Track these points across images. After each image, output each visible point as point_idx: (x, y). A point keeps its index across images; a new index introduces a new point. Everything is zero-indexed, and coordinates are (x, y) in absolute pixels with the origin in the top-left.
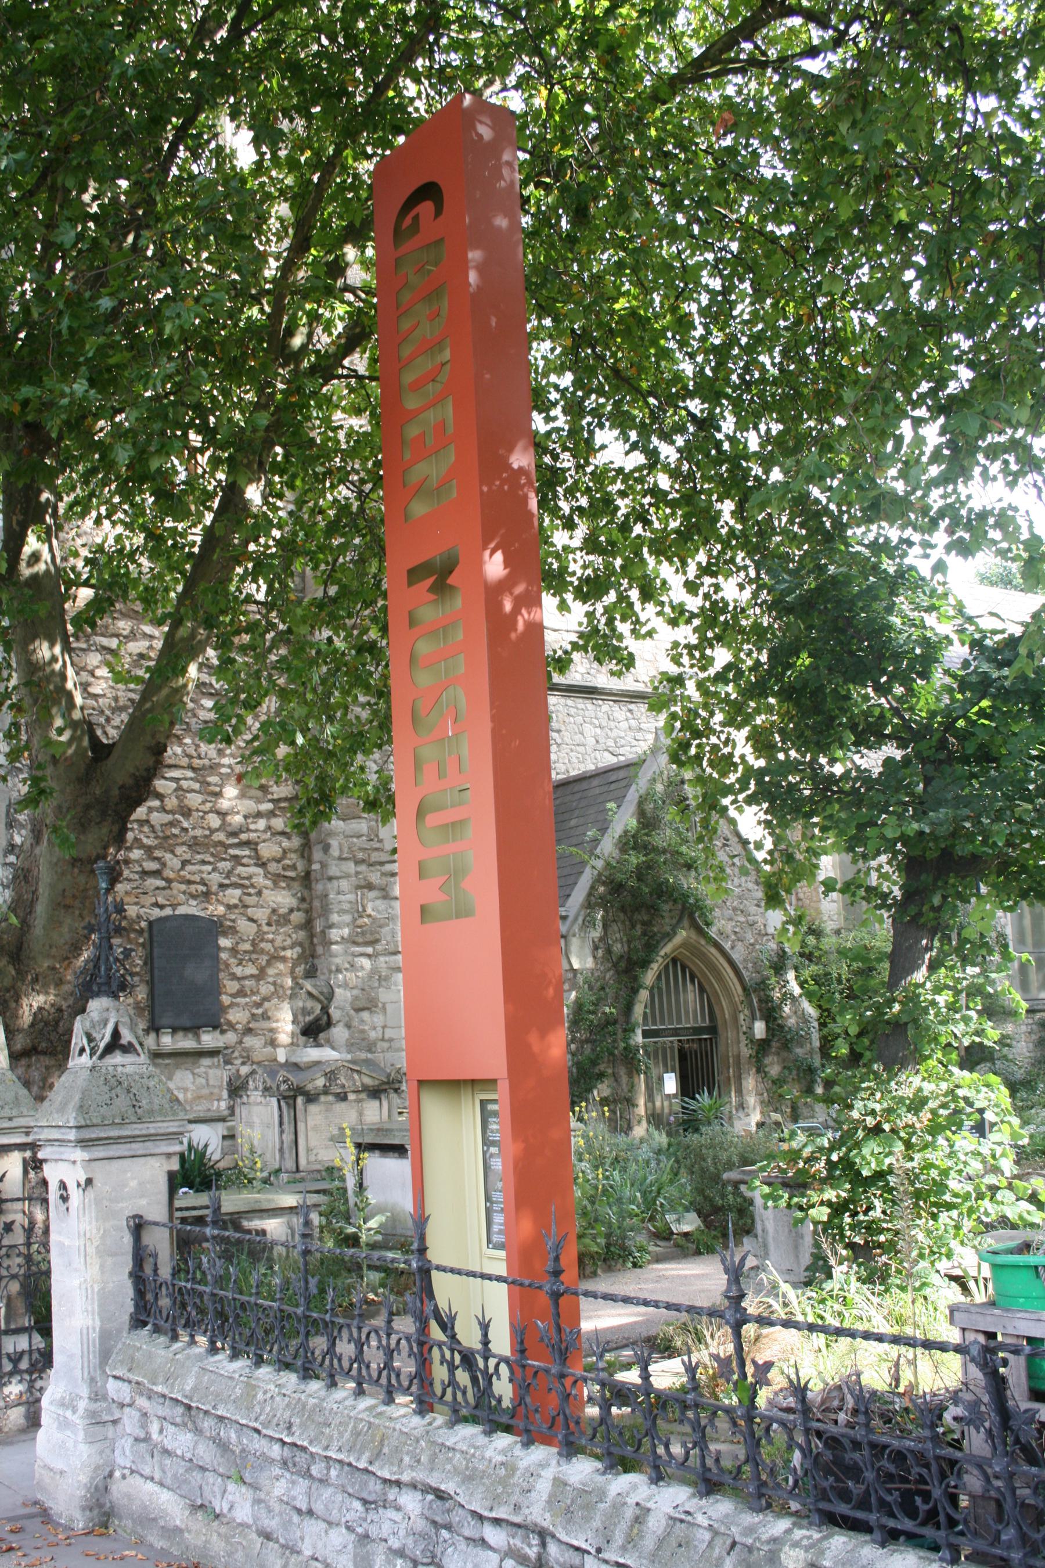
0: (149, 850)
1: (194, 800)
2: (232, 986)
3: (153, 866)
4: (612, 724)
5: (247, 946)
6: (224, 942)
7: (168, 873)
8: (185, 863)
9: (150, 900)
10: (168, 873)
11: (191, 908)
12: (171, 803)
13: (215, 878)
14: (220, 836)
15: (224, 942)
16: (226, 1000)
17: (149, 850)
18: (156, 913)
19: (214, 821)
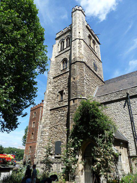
0: (56, 134)
1: (60, 128)
2: (63, 149)
3: (56, 136)
4: (117, 105)
5: (64, 144)
6: (62, 144)
7: (58, 136)
8: (59, 135)
9: (56, 139)
10: (58, 136)
11: (59, 140)
12: (58, 129)
13: (62, 136)
14: (62, 132)
15: (62, 144)
16: (62, 151)
17: (56, 134)
18: (56, 141)
19: (62, 130)
